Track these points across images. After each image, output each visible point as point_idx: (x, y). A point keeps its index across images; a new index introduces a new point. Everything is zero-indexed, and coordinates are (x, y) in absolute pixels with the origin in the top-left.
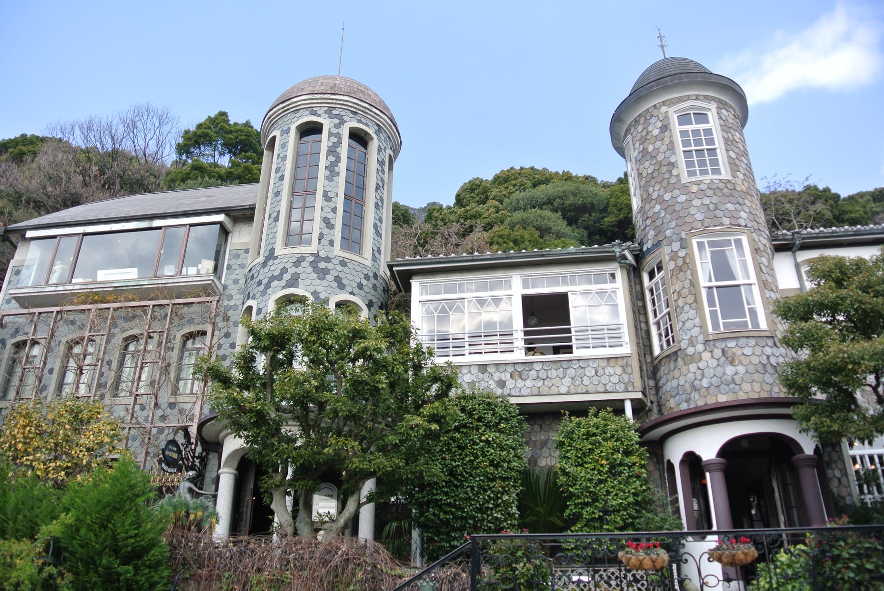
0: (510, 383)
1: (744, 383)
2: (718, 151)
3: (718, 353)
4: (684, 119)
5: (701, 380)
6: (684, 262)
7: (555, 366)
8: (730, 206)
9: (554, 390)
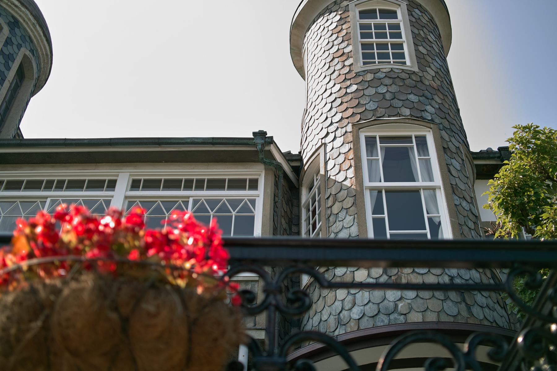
1: (412, 311)
2: (405, 46)
5: (350, 309)
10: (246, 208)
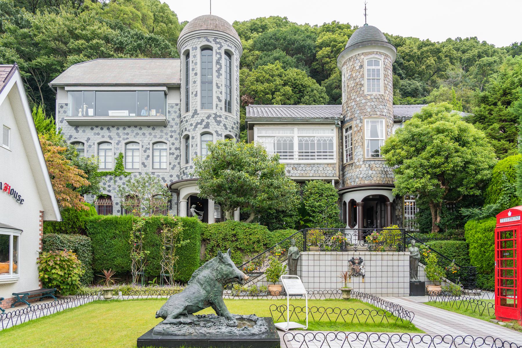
0: (292, 172)
3: (367, 165)
4: (370, 63)
6: (360, 129)
7: (309, 166)
8: (381, 107)
9: (308, 175)
10: (331, 140)
